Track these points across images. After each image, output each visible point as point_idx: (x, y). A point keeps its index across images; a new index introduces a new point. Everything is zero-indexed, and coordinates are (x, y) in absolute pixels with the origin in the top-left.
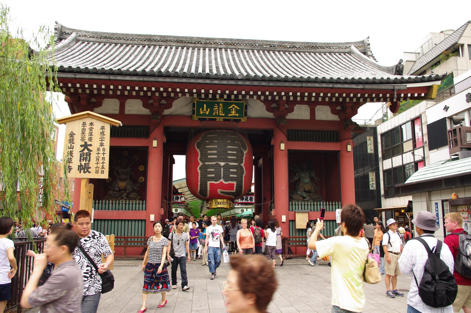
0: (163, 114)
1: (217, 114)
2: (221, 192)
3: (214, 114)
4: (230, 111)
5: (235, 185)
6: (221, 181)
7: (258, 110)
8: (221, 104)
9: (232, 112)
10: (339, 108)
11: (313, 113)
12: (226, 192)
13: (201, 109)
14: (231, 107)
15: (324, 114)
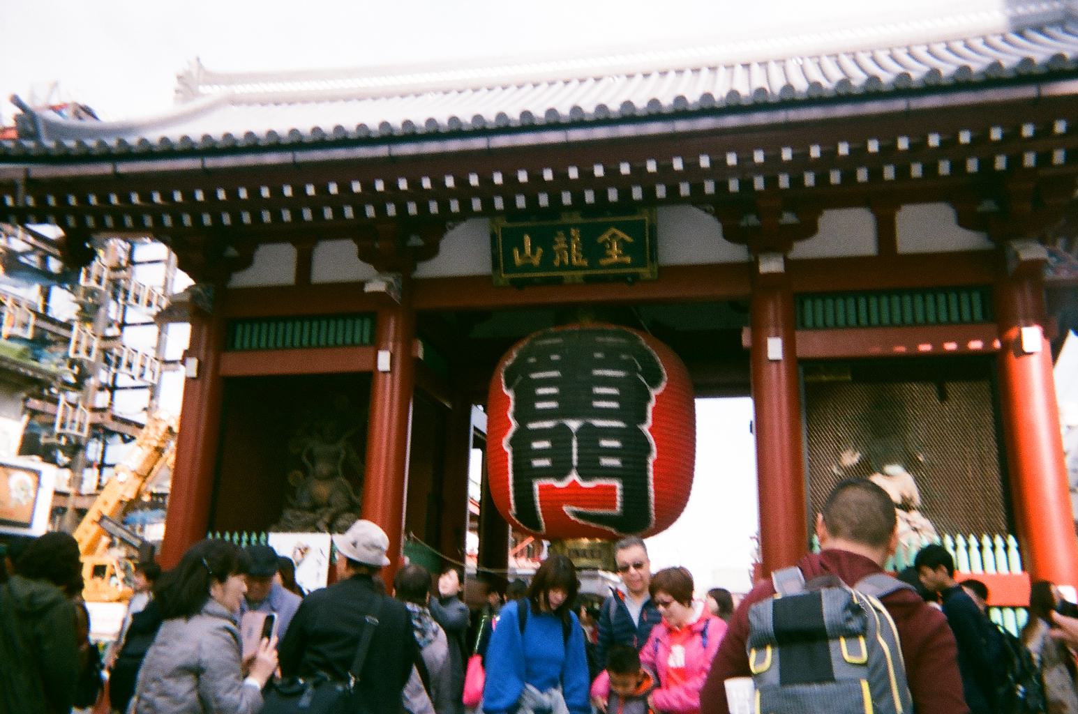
1: (567, 261)
3: (557, 263)
4: (602, 251)
7: (695, 241)
8: (573, 232)
9: (609, 252)
10: (988, 206)
11: (886, 232)
13: (516, 252)
14: (606, 236)
15: (929, 229)
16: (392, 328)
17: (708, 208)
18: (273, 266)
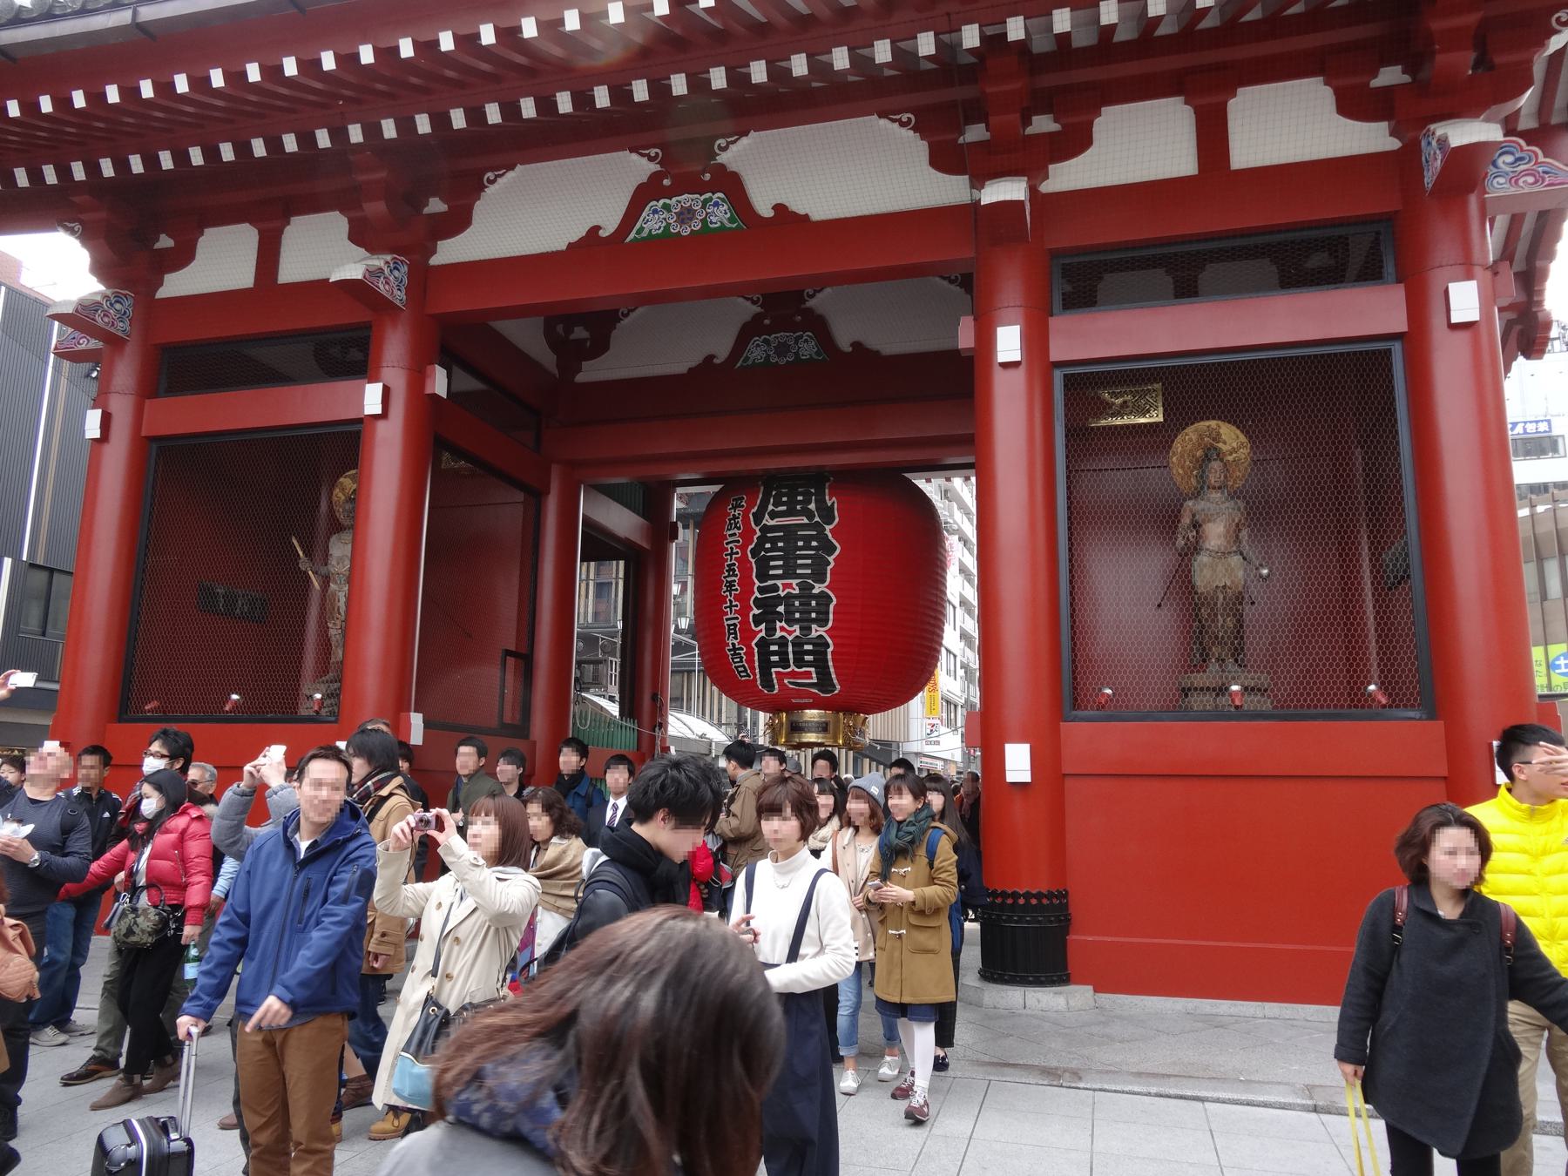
0: (435, 261)
11: (1212, 136)
16: (394, 349)
17: (905, 117)
18: (221, 263)
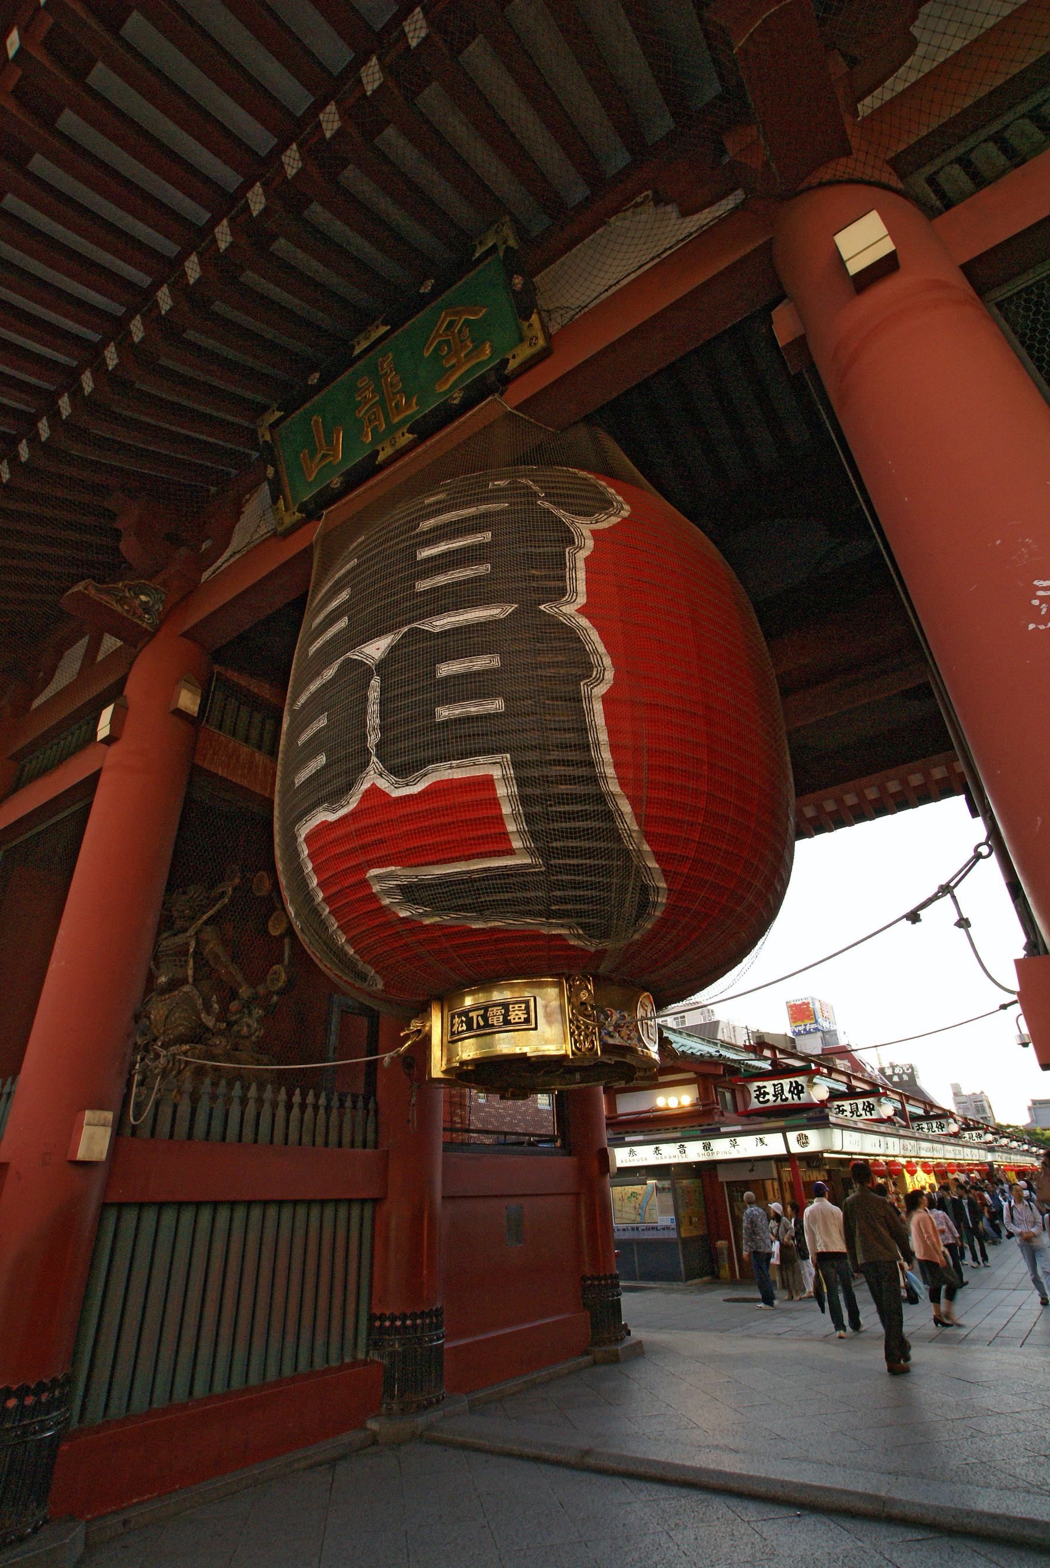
2: (401, 888)
5: (501, 791)
6: (366, 786)
12: (445, 882)
